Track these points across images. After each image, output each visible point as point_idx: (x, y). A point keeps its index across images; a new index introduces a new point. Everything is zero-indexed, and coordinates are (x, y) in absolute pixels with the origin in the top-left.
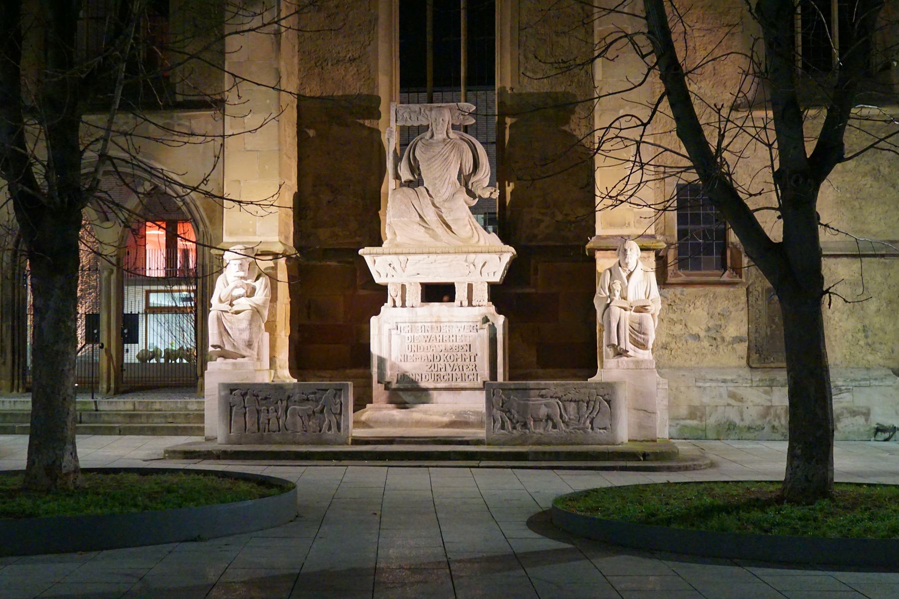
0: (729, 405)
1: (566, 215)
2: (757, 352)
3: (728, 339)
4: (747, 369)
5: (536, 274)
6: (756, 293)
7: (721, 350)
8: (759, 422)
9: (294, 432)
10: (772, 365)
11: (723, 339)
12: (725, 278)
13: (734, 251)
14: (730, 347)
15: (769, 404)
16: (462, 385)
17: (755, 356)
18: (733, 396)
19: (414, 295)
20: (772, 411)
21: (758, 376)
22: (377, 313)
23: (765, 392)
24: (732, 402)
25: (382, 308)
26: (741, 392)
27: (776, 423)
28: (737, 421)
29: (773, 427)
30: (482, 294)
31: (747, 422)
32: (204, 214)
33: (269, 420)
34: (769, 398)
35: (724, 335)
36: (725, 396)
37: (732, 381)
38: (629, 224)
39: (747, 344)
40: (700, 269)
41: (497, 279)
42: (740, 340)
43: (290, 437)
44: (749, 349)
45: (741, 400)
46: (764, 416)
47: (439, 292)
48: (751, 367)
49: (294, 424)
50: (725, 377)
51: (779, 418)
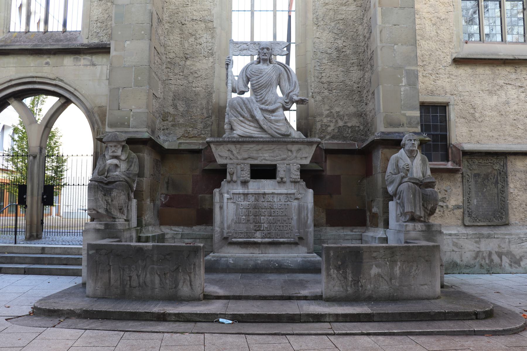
0: (453, 251)
1: (346, 123)
2: (470, 215)
3: (450, 206)
4: (462, 227)
5: (326, 161)
6: (467, 176)
7: (446, 214)
8: (472, 262)
9: (153, 289)
10: (479, 224)
11: (447, 206)
12: (449, 165)
13: (454, 149)
14: (451, 213)
15: (478, 250)
16: (282, 240)
17: (467, 219)
18: (455, 244)
19: (246, 174)
20: (480, 254)
21: (470, 231)
22: (219, 186)
23: (476, 242)
24: (455, 249)
25: (222, 183)
26: (461, 242)
27: (483, 262)
28: (458, 261)
29: (481, 266)
30: (296, 175)
31: (464, 263)
32: (98, 118)
33: (130, 277)
34: (478, 246)
35: (448, 204)
36: (451, 244)
37: (455, 235)
38: (403, 125)
39: (462, 210)
40: (431, 161)
41: (307, 162)
42: (458, 207)
43: (149, 293)
44: (463, 213)
45: (461, 247)
46: (475, 258)
47: (264, 172)
48: (465, 226)
49: (153, 282)
50: (450, 232)
51: (485, 259)
